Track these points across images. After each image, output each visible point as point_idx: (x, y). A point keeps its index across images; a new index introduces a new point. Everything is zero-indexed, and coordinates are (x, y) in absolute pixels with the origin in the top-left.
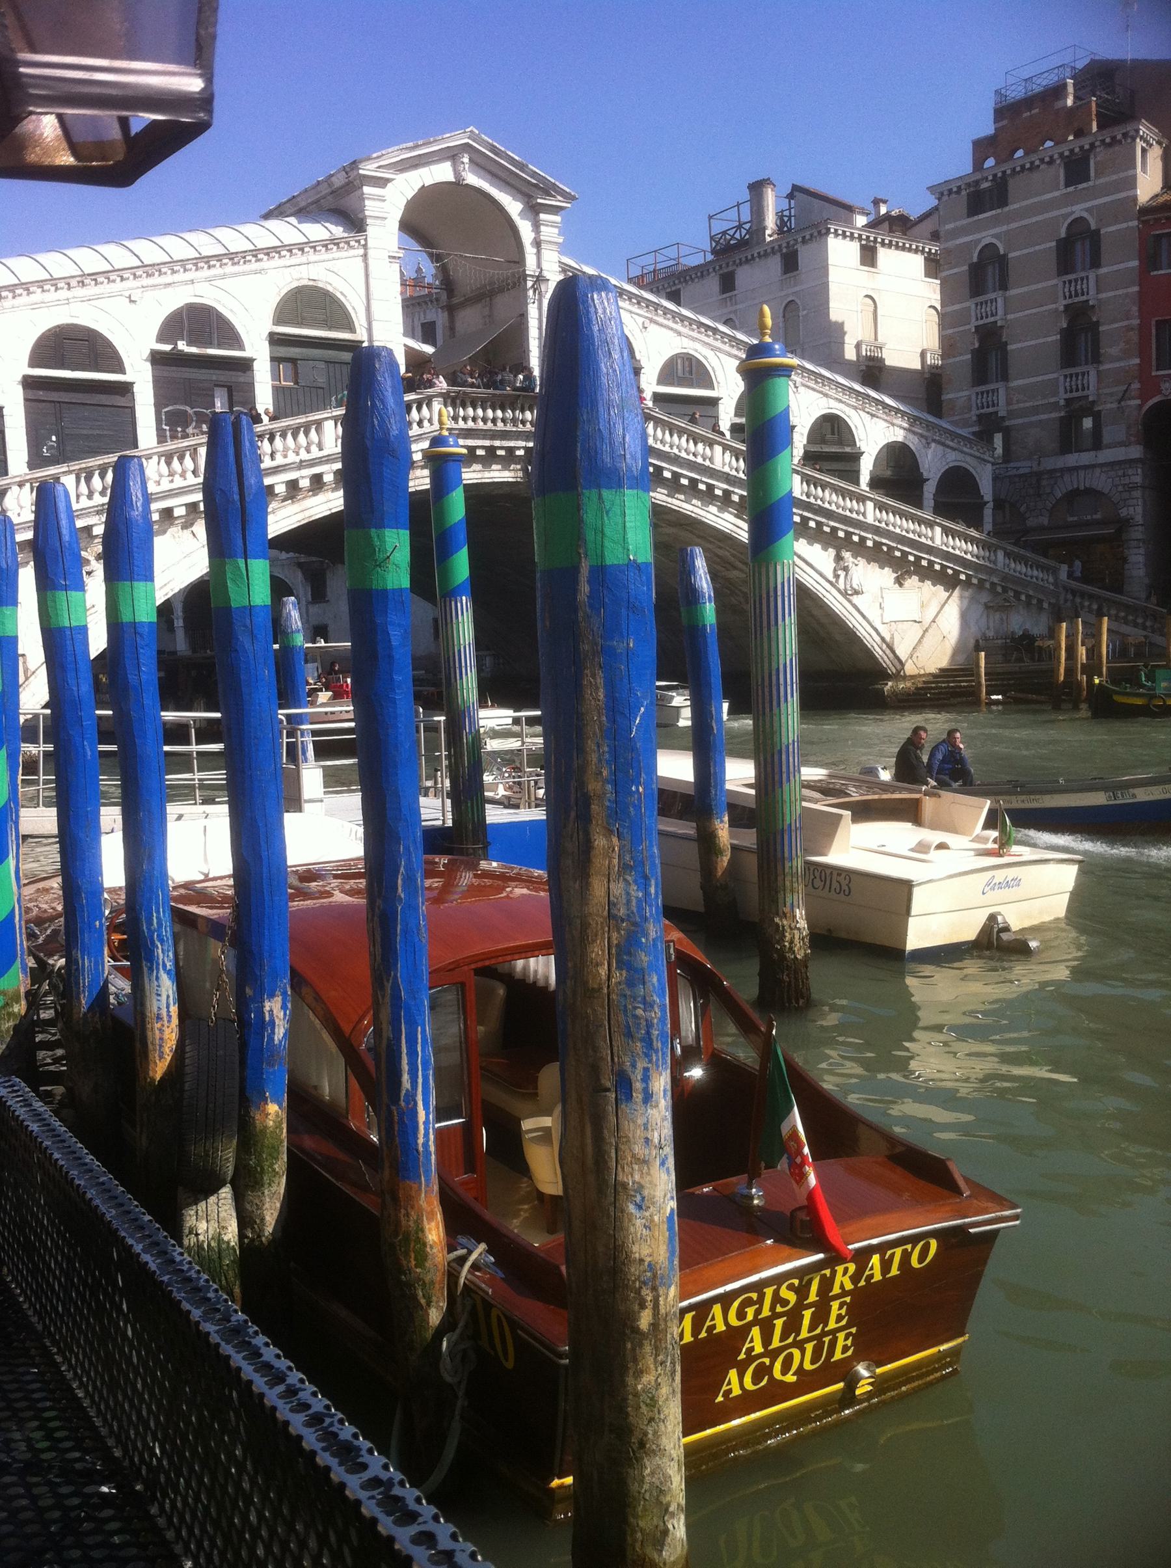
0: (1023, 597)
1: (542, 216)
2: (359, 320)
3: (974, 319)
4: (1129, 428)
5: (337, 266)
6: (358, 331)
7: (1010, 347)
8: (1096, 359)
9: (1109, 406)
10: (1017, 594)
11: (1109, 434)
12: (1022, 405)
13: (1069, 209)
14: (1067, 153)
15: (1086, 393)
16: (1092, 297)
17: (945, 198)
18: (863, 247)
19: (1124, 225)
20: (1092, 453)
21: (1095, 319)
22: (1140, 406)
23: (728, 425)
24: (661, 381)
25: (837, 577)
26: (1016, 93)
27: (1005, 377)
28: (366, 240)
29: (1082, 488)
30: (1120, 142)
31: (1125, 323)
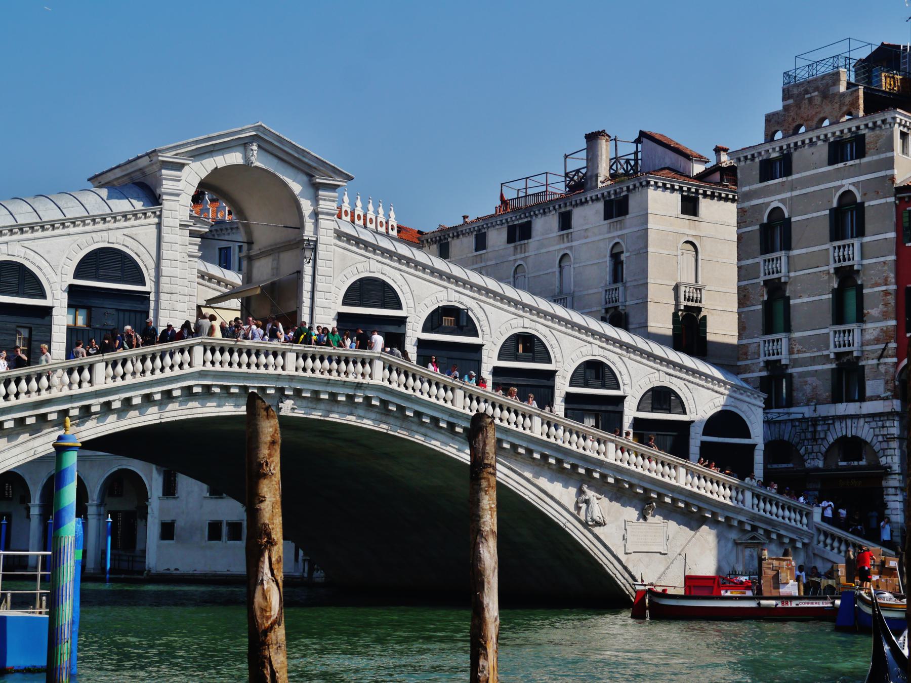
0: (774, 536)
1: (321, 193)
2: (149, 275)
3: (762, 274)
4: (887, 383)
7: (792, 302)
8: (861, 318)
9: (870, 362)
10: (767, 533)
11: (873, 386)
12: (801, 355)
18: (683, 197)
19: (883, 201)
20: (858, 404)
21: (859, 282)
22: (897, 364)
23: (490, 368)
24: (425, 329)
25: (578, 508)
26: (803, 75)
27: (788, 329)
28: (161, 211)
31: (884, 288)
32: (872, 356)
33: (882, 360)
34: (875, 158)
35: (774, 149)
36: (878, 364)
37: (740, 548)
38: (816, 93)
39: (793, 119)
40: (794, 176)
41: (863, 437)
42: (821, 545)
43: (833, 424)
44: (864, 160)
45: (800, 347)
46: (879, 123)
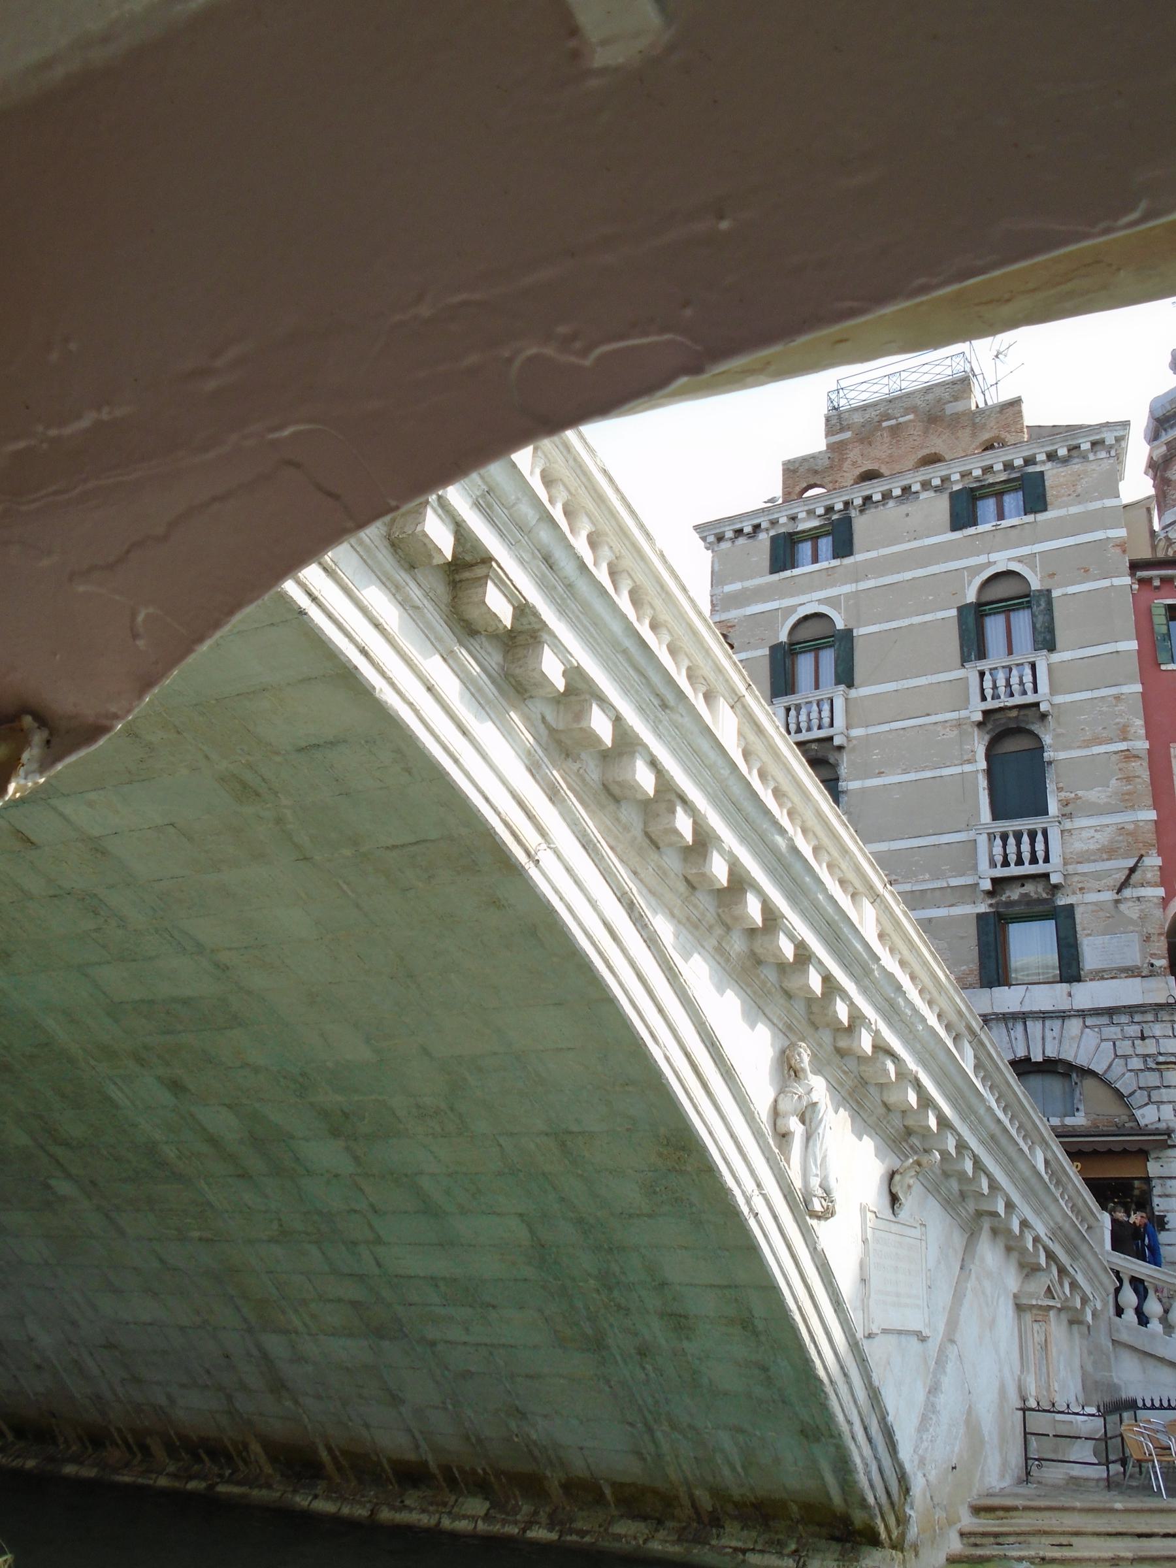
4: (1147, 939)
9: (1092, 897)
11: (1092, 952)
13: (982, 559)
15: (1040, 868)
17: (725, 545)
19: (1105, 583)
25: (784, 1137)
29: (1037, 1057)
30: (1085, 458)
31: (1122, 746)
32: (1097, 885)
33: (1127, 893)
34: (1073, 510)
35: (811, 513)
36: (1117, 902)
37: (1028, 1317)
38: (911, 417)
39: (854, 463)
40: (858, 557)
41: (1082, 1060)
42: (1130, 1316)
44: (1041, 517)
46: (1085, 446)
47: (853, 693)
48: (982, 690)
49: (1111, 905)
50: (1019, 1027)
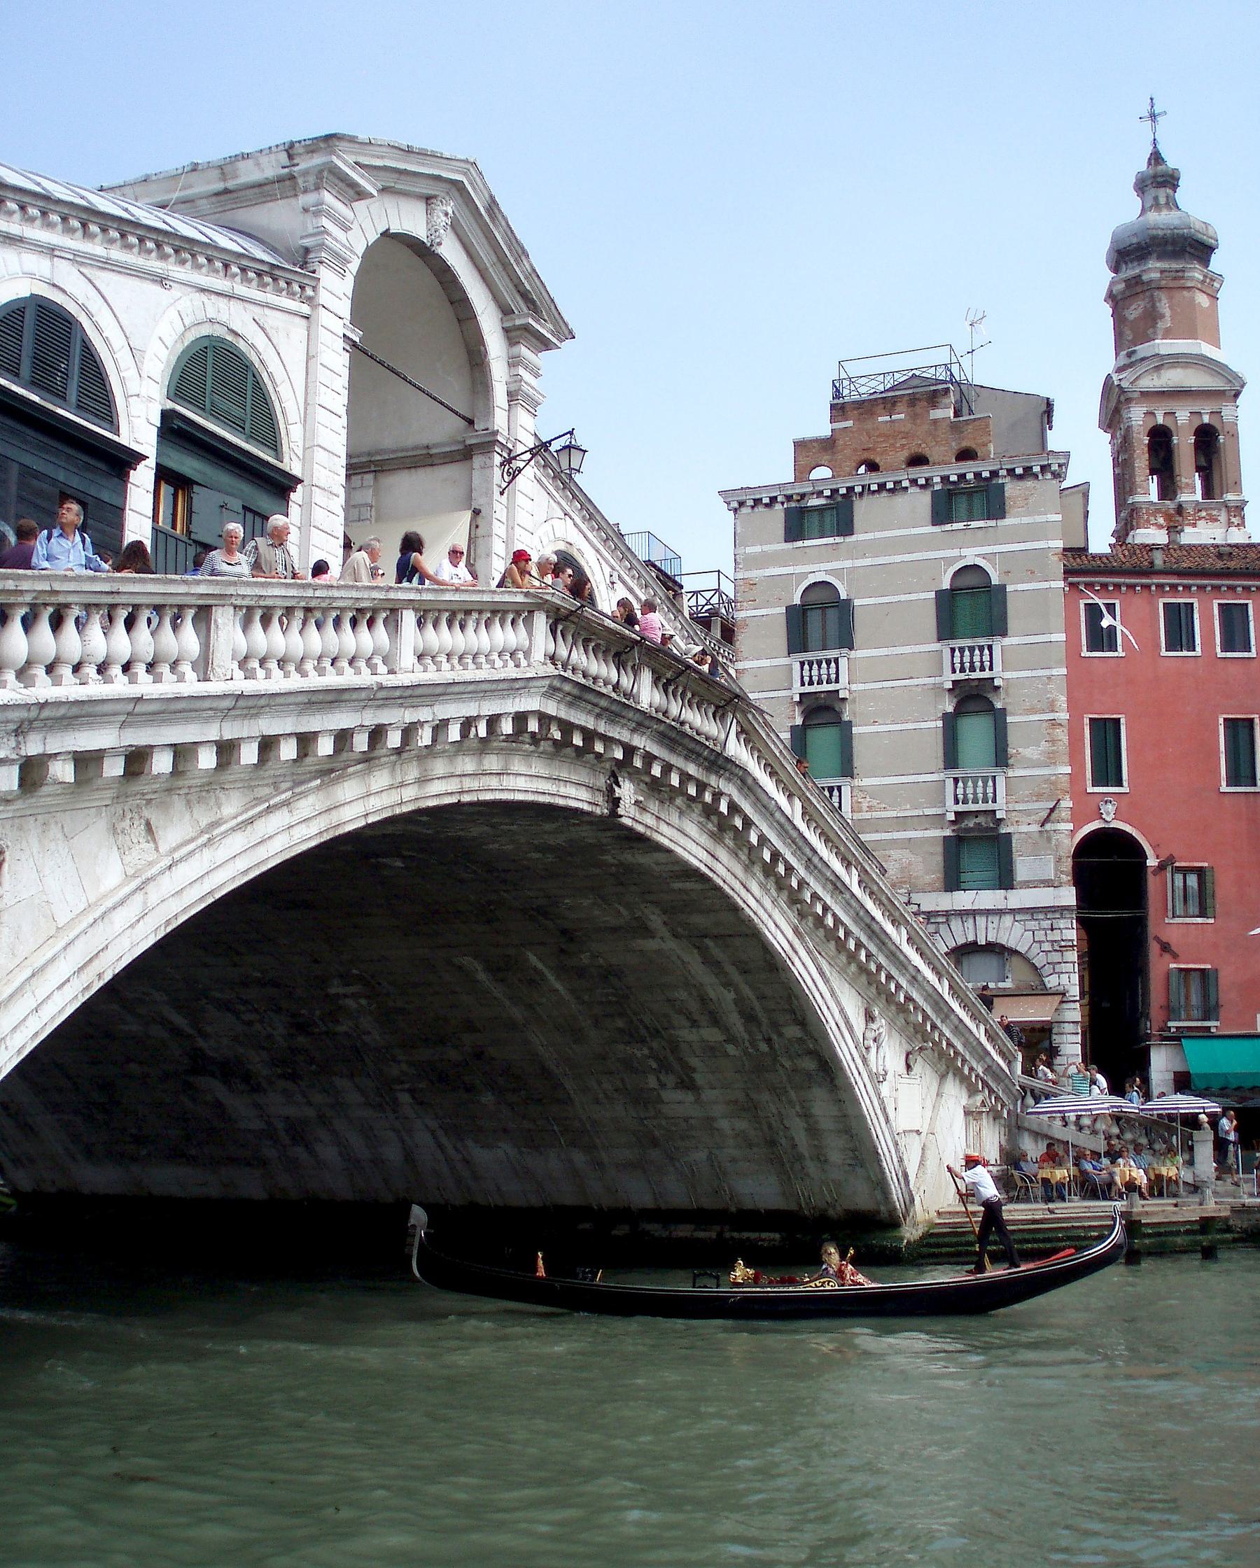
3: (797, 683)
4: (1059, 860)
5: (273, 320)
6: (286, 459)
7: (855, 730)
8: (1001, 758)
9: (1024, 828)
11: (1023, 868)
13: (955, 553)
14: (954, 478)
16: (1000, 675)
17: (744, 510)
19: (1045, 585)
21: (998, 705)
33: (1048, 827)
34: (1025, 520)
41: (1011, 944)
43: (947, 922)
45: (875, 802)
46: (1036, 469)
47: (853, 654)
48: (953, 664)
49: (1037, 835)
50: (971, 921)
